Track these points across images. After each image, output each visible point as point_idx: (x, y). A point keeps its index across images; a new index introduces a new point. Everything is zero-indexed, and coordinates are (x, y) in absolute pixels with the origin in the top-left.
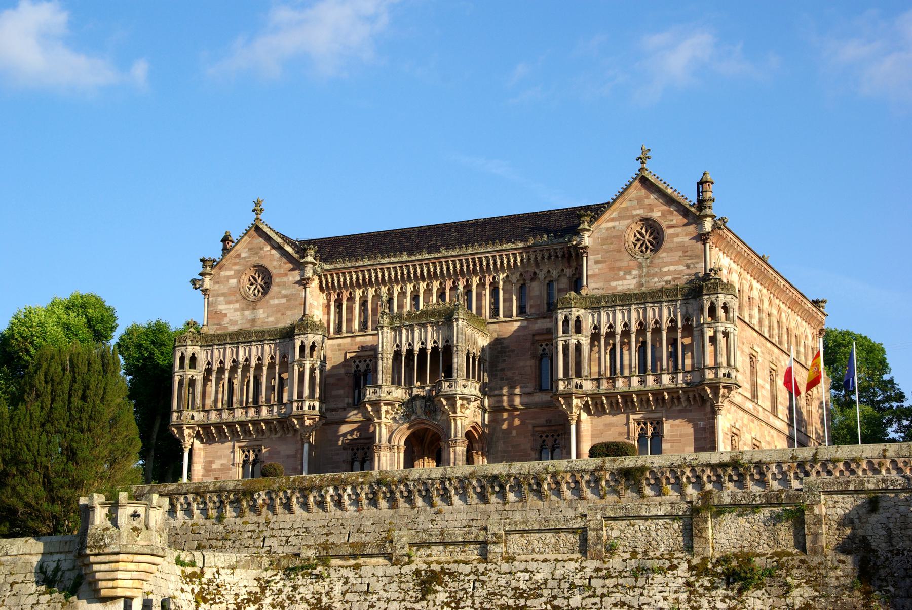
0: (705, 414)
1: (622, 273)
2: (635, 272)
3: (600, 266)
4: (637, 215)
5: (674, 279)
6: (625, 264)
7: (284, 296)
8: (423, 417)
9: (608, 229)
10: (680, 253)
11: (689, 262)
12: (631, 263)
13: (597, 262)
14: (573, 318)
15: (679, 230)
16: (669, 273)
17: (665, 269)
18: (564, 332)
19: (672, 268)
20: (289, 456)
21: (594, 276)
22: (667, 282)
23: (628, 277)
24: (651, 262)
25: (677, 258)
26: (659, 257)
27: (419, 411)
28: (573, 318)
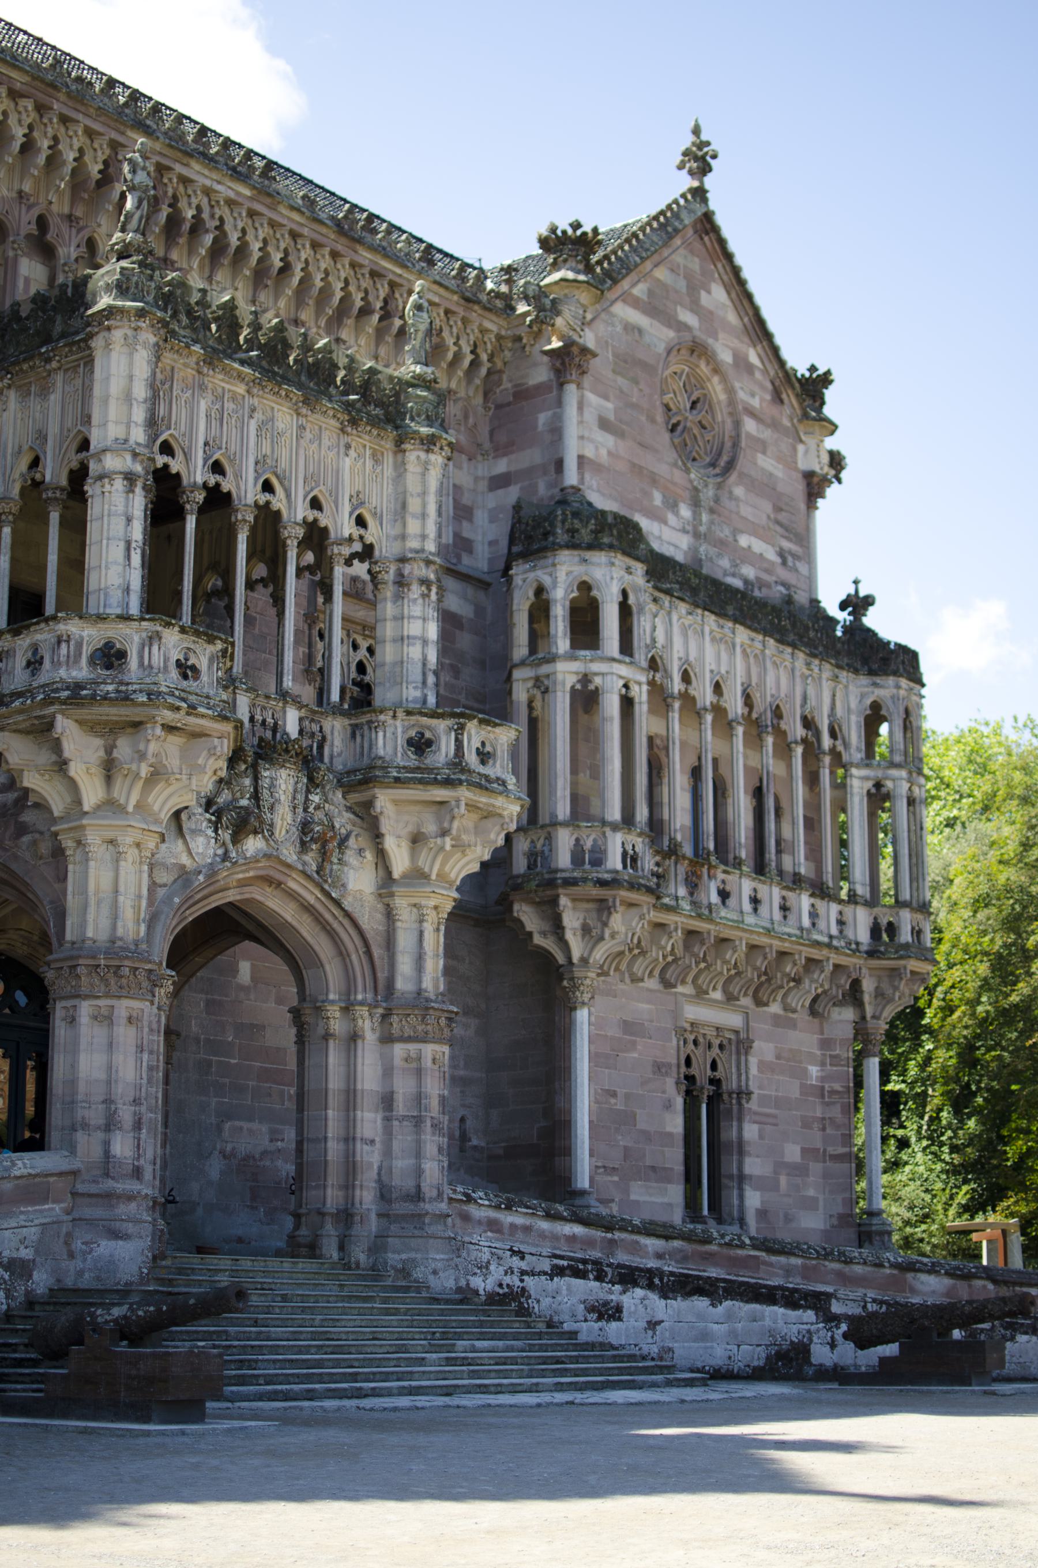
0: (826, 1044)
1: (658, 498)
2: (685, 512)
3: (609, 440)
4: (687, 327)
5: (762, 584)
6: (662, 469)
8: (290, 854)
9: (630, 328)
10: (767, 507)
11: (786, 545)
12: (678, 476)
13: (604, 424)
14: (561, 597)
15: (767, 434)
16: (747, 556)
17: (744, 541)
18: (575, 645)
19: (758, 546)
21: (598, 467)
22: (746, 582)
23: (671, 518)
24: (717, 500)
25: (764, 520)
26: (731, 496)
27: (284, 820)
28: (561, 597)
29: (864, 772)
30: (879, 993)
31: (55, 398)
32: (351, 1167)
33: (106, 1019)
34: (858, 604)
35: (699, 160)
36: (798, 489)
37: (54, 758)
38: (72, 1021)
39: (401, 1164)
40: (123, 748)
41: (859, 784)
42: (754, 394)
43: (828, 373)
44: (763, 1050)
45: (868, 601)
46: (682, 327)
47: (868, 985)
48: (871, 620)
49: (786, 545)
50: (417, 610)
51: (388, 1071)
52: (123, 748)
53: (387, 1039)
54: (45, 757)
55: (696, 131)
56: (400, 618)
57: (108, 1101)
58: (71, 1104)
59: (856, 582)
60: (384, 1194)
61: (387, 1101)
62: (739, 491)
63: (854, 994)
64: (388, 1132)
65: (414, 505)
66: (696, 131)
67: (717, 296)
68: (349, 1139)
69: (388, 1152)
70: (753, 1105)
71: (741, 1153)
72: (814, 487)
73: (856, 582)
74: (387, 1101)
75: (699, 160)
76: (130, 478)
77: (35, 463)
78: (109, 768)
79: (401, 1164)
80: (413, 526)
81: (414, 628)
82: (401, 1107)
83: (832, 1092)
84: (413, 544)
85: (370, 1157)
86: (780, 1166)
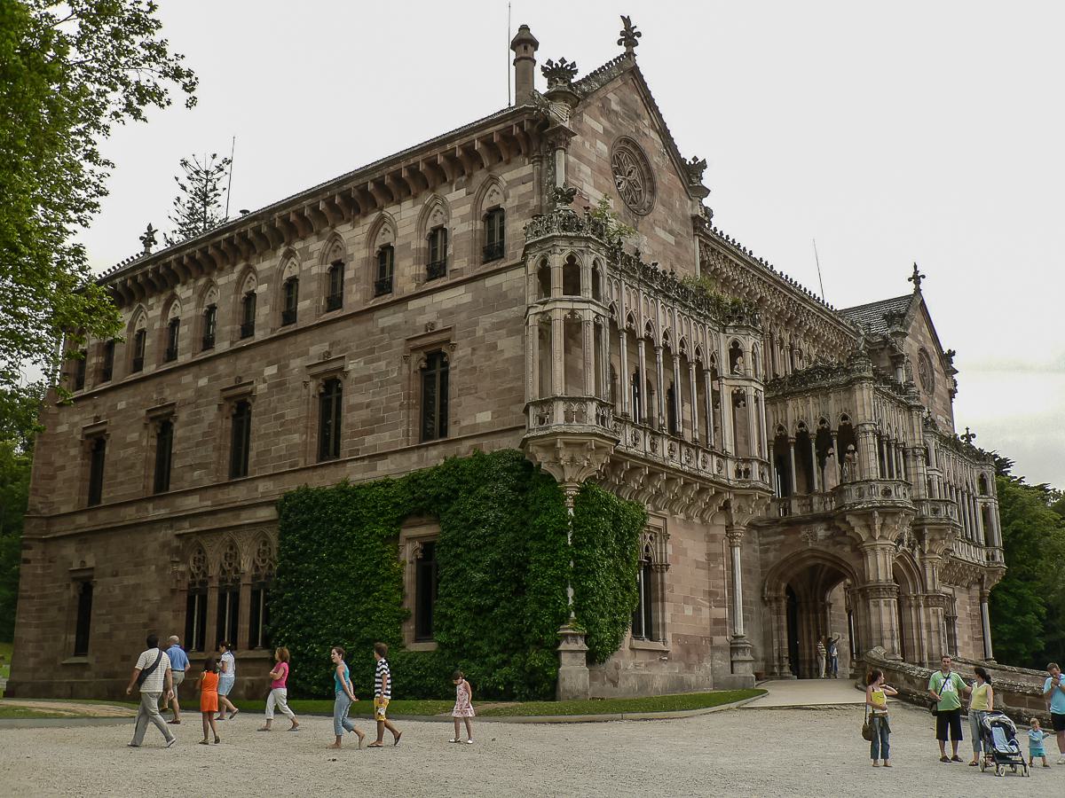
0: (970, 598)
7: (671, 232)
11: (948, 417)
20: (698, 565)
26: (935, 402)
29: (981, 500)
30: (989, 579)
31: (832, 402)
32: (921, 648)
33: (888, 605)
34: (969, 437)
35: (916, 278)
36: (947, 396)
37: (864, 523)
38: (877, 605)
39: (935, 647)
40: (889, 521)
41: (979, 506)
42: (936, 362)
43: (954, 352)
44: (957, 603)
45: (974, 436)
46: (919, 341)
47: (985, 577)
48: (974, 442)
49: (948, 417)
50: (921, 464)
51: (928, 616)
52: (889, 521)
53: (927, 606)
54: (862, 523)
55: (915, 267)
56: (917, 467)
57: (892, 630)
58: (881, 631)
59: (967, 429)
60: (931, 657)
61: (929, 626)
62: (936, 399)
63: (980, 582)
64: (930, 637)
65: (916, 428)
66: (915, 267)
67: (925, 329)
68: (920, 639)
69: (930, 643)
70: (957, 621)
71: (955, 638)
72: (952, 393)
73: (967, 429)
74: (929, 626)
75: (916, 278)
76: (873, 431)
77: (823, 421)
78: (883, 525)
79: (935, 647)
80: (917, 436)
81: (921, 470)
82: (933, 629)
83: (974, 615)
84: (917, 442)
85: (925, 643)
86: (964, 642)
